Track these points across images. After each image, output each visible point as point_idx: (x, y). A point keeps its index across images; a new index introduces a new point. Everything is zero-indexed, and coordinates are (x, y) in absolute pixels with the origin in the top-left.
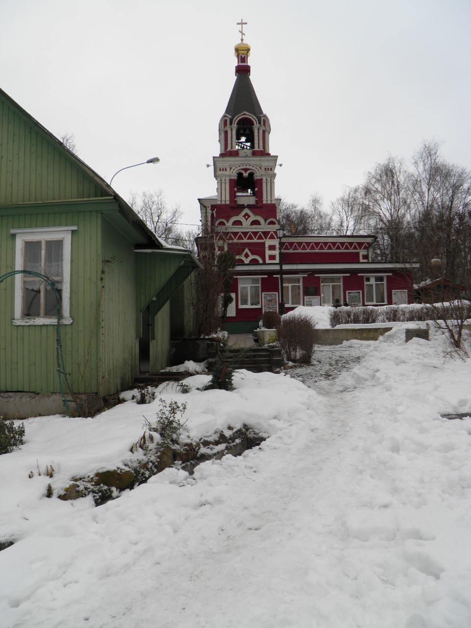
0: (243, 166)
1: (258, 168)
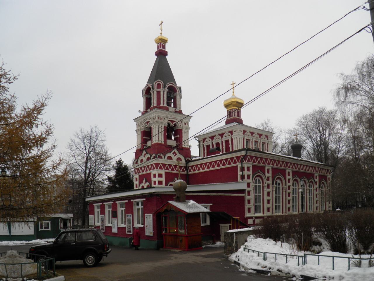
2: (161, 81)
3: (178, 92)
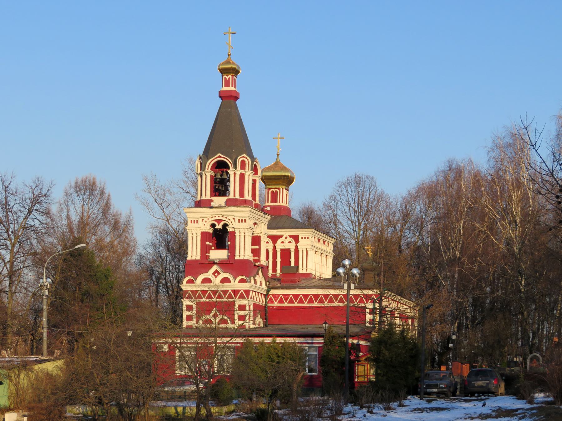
0: (215, 217)
1: (232, 219)
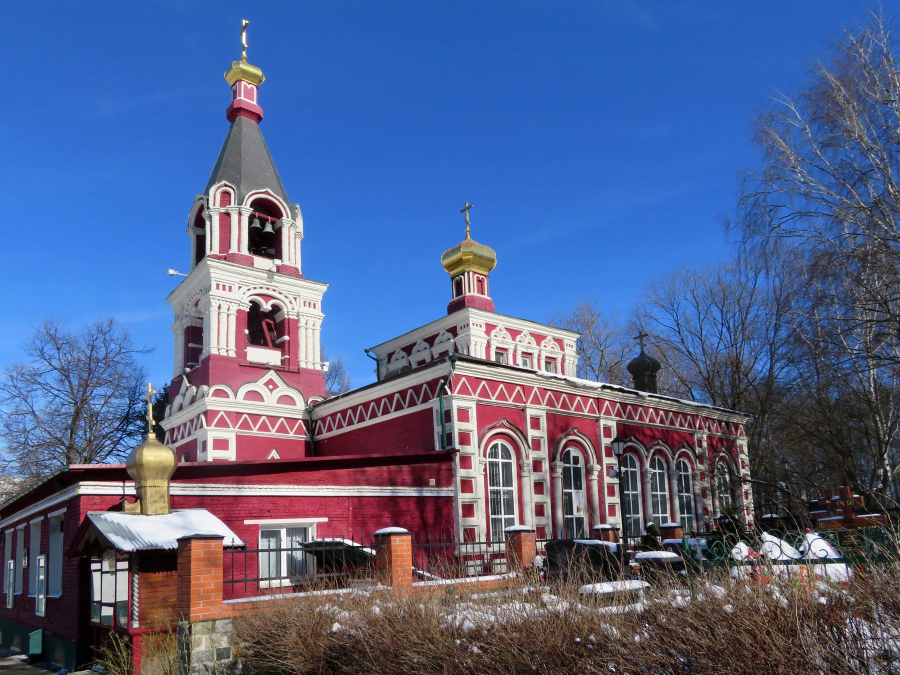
1: (291, 297)
2: (230, 185)
3: (285, 217)
